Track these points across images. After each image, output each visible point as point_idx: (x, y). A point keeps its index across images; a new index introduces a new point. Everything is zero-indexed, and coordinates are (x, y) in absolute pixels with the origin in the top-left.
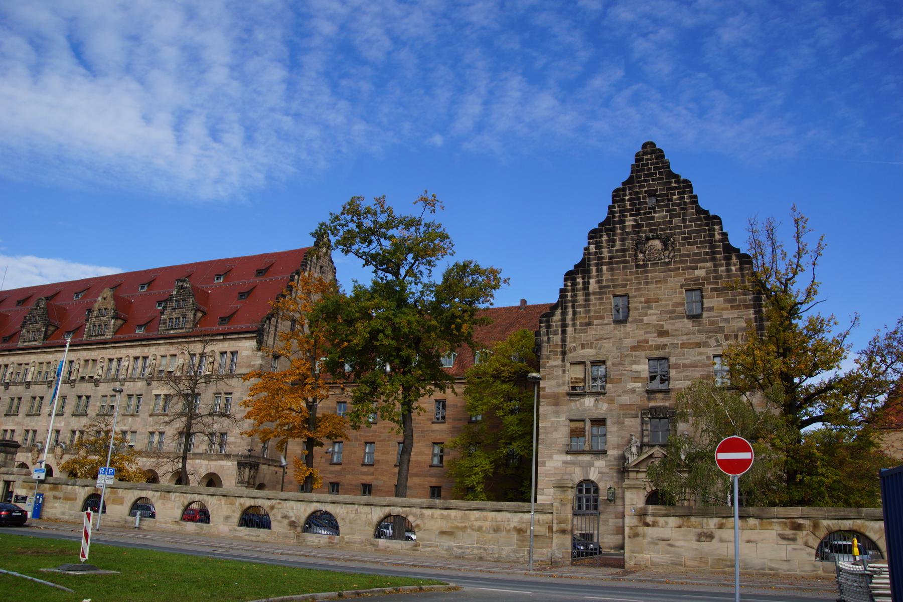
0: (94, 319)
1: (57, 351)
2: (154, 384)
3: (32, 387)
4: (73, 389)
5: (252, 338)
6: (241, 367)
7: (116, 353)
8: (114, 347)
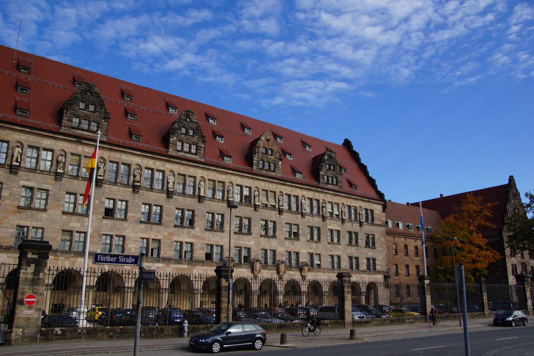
0: (261, 155)
2: (327, 220)
3: (207, 203)
4: (257, 213)
5: (380, 204)
6: (377, 220)
7: (292, 191)
8: (291, 186)
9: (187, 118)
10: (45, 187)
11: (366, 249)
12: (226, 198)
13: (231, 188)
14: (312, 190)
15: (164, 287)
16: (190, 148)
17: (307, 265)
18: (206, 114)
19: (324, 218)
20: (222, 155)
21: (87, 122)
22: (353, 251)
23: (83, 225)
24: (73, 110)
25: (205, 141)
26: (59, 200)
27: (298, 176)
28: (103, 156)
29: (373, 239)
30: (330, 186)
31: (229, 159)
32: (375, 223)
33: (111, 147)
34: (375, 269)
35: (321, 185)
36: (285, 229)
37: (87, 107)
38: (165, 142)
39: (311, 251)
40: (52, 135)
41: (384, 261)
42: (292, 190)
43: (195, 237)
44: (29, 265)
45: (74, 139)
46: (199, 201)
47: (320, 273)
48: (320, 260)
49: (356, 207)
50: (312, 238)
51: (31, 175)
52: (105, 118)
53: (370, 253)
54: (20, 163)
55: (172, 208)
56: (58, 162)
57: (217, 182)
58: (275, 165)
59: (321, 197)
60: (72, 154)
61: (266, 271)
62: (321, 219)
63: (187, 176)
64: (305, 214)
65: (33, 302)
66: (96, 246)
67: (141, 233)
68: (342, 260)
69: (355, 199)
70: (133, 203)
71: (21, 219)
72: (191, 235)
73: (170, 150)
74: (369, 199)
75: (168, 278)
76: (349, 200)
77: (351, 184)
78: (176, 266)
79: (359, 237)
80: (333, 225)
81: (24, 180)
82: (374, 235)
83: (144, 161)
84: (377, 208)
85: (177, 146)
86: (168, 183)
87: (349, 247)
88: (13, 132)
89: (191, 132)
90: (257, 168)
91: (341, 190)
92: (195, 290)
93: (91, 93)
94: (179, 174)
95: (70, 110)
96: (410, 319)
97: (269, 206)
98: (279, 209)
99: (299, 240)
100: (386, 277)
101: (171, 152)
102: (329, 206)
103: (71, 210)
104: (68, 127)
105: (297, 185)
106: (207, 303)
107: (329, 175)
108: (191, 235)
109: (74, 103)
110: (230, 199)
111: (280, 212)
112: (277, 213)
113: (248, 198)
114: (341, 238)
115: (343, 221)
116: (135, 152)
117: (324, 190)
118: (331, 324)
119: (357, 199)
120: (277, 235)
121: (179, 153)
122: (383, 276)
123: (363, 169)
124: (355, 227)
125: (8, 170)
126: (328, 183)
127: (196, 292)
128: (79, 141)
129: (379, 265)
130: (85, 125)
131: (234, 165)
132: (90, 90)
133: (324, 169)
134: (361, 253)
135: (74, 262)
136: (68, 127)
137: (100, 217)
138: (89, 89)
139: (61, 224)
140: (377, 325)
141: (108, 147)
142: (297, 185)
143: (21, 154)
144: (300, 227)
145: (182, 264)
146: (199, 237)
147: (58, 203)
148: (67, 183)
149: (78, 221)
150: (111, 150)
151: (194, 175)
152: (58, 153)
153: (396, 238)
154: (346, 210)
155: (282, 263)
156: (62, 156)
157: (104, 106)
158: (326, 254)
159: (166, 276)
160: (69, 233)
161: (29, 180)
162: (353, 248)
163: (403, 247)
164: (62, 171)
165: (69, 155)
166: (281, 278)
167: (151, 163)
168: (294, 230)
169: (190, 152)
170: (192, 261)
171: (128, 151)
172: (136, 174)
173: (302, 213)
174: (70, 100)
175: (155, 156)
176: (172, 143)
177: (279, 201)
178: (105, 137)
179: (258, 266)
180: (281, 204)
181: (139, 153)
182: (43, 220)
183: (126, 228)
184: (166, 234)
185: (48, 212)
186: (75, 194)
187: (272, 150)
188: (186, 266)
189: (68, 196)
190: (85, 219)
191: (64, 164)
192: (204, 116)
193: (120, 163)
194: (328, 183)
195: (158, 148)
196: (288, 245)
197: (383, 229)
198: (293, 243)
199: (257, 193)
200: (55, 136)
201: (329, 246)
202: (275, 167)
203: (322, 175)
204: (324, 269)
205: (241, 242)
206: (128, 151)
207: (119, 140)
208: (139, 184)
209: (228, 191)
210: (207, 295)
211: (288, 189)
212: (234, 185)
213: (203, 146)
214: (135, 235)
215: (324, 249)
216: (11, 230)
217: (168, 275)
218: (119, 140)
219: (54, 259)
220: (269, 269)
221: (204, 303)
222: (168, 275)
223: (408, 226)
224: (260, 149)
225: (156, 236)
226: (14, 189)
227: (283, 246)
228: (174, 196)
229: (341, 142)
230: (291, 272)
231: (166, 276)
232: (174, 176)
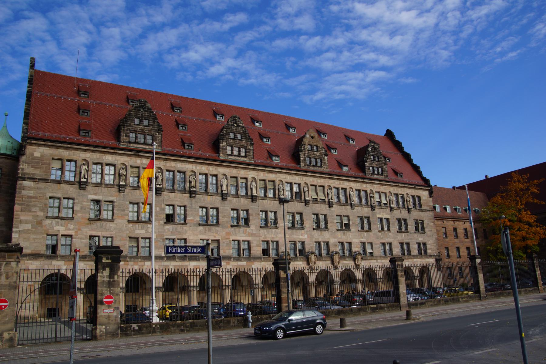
0: (307, 152)
1: (280, 172)
2: (376, 209)
3: (259, 201)
4: (308, 208)
6: (424, 206)
7: (340, 184)
8: (338, 179)
9: (234, 123)
11: (416, 235)
12: (277, 196)
13: (281, 186)
14: (358, 182)
15: (227, 284)
16: (239, 151)
17: (359, 254)
18: (251, 118)
19: (373, 208)
20: (270, 155)
21: (142, 136)
22: (403, 237)
23: (147, 232)
25: (253, 144)
26: (124, 210)
27: (344, 169)
29: (422, 224)
30: (376, 177)
31: (277, 158)
32: (422, 208)
34: (426, 253)
35: (367, 176)
36: (336, 221)
37: (141, 122)
38: (216, 148)
39: (363, 240)
40: (112, 151)
41: (435, 245)
42: (340, 183)
43: (251, 235)
45: (133, 153)
46: (252, 201)
47: (372, 261)
48: (372, 248)
49: (403, 195)
50: (363, 228)
51: (98, 189)
52: (159, 130)
53: (421, 238)
54: (87, 179)
55: (227, 210)
56: (120, 175)
57: (267, 181)
58: (321, 160)
59: (368, 187)
60: (132, 167)
61: (321, 263)
62: (370, 209)
63: (239, 178)
64: (355, 205)
67: (200, 235)
68: (393, 246)
69: (401, 187)
70: (190, 207)
71: (92, 230)
72: (247, 234)
73: (221, 155)
74: (415, 186)
75: (229, 274)
76: (395, 188)
77: (396, 173)
78: (235, 263)
79: (408, 224)
80: (382, 213)
81: (91, 195)
82: (422, 221)
83: (198, 168)
84: (424, 194)
85: (227, 150)
86: (222, 186)
87: (399, 234)
88: (79, 152)
89: (239, 136)
90: (305, 165)
91: (387, 179)
92: (256, 285)
93: (143, 109)
94: (231, 177)
96: (464, 298)
97: (319, 200)
98: (329, 202)
99: (350, 230)
100: (438, 261)
101: (222, 156)
102: (376, 196)
103: (135, 219)
104: (126, 142)
105: (344, 178)
106: (268, 296)
107: (375, 166)
108: (247, 234)
109: (130, 120)
110: (281, 197)
111: (330, 205)
112: (327, 206)
113: (298, 194)
114: (391, 225)
115: (391, 209)
116: (188, 160)
117: (371, 180)
118: (387, 307)
119: (404, 187)
120: (328, 227)
121: (230, 157)
122: (434, 259)
123: (407, 157)
124: (404, 214)
125: (78, 187)
126: (374, 173)
127: (257, 286)
129: (430, 249)
131: (282, 164)
132: (142, 106)
133: (369, 161)
134: (411, 239)
135: (142, 266)
137: (162, 222)
138: (142, 105)
139: (128, 232)
140: (432, 306)
141: (163, 157)
142: (344, 178)
143: (88, 171)
144: (350, 218)
145: (241, 261)
146: (255, 234)
147: (123, 213)
148: (130, 194)
149: (143, 228)
150: (167, 160)
151: (246, 176)
152: (120, 167)
153: (445, 221)
154: (394, 198)
155: (336, 253)
156: (123, 169)
157: (157, 119)
158: (378, 242)
159: (228, 272)
160: (136, 240)
162: (403, 235)
163: (452, 230)
164: (124, 184)
165: (129, 168)
166: (336, 268)
167: (204, 169)
168: (345, 221)
169: (239, 155)
170: (250, 258)
171: (182, 159)
172: (191, 180)
173: (351, 204)
174: (125, 118)
175: (208, 162)
176: (222, 149)
177: (328, 194)
179: (313, 258)
180: (330, 198)
181: (193, 160)
183: (186, 231)
184: (224, 234)
185: (115, 222)
186: (138, 204)
187: (317, 147)
188: (244, 263)
189: (131, 205)
190: (149, 226)
191: (126, 176)
192: (250, 120)
193: (176, 172)
194: (374, 173)
195: (210, 154)
196: (340, 236)
197: (431, 214)
198: (344, 234)
199: (306, 189)
200: (116, 151)
201: (380, 234)
202: (321, 163)
203: (368, 166)
204: (376, 257)
205: (295, 236)
206: (182, 159)
207: (173, 149)
208: (195, 189)
209: (279, 189)
210: (268, 289)
211: (336, 183)
212: (284, 182)
213: (251, 148)
214: (195, 237)
215: (374, 237)
216: (85, 240)
217: (229, 270)
218: (173, 149)
219: (125, 264)
220: (324, 261)
221: (265, 297)
222: (229, 270)
223: (456, 209)
224: (306, 146)
225: (215, 236)
226: (84, 203)
227: (334, 238)
228: (229, 198)
229: (383, 133)
230: (345, 262)
231: (228, 272)
232: (227, 179)
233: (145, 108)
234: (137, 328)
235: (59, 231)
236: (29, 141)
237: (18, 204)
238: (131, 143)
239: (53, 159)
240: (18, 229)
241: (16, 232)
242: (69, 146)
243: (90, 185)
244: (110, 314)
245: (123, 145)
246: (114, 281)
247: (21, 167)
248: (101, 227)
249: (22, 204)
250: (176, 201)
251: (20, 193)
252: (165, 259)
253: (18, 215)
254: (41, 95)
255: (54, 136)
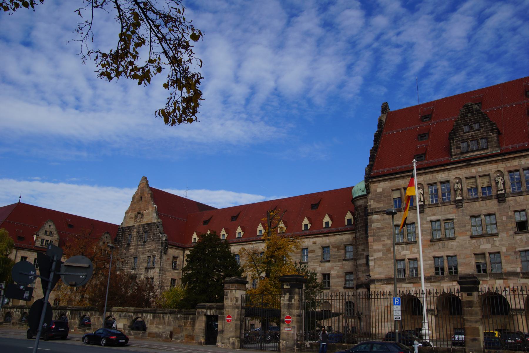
10: (449, 216)
23: (494, 245)
24: (458, 137)
26: (465, 226)
28: (499, 169)
33: (503, 157)
37: (471, 128)
40: (443, 168)
44: (285, 294)
45: (464, 164)
51: (435, 210)
52: (492, 130)
54: (424, 202)
60: (467, 178)
65: (290, 321)
66: (514, 265)
71: (435, 251)
75: (344, 297)
95: (456, 137)
104: (458, 154)
109: (458, 130)
128: (469, 163)
130: (473, 145)
132: (469, 111)
136: (458, 154)
137: (511, 233)
139: (472, 248)
141: (500, 158)
143: (423, 194)
147: (463, 229)
149: (488, 242)
150: (506, 160)
156: (457, 183)
157: (488, 118)
159: (342, 296)
160: (483, 256)
161: (434, 215)
164: (461, 198)
165: (464, 180)
174: (453, 129)
178: (497, 149)
182: (454, 248)
185: (457, 239)
191: (461, 190)
216: (429, 262)
217: (344, 294)
222: (344, 294)
226: (424, 226)
231: (342, 296)
233: (473, 112)
234: (309, 346)
235: (405, 255)
236: (370, 180)
237: (371, 236)
238: (463, 153)
239: (393, 190)
240: (373, 258)
241: (372, 260)
242: (402, 175)
243: (427, 207)
244: (289, 332)
245: (455, 158)
246: (292, 304)
247: (369, 204)
248: (443, 247)
249: (374, 236)
250: (526, 205)
251: (371, 226)
252: (521, 275)
253: (372, 245)
254: (389, 134)
255: (392, 169)
